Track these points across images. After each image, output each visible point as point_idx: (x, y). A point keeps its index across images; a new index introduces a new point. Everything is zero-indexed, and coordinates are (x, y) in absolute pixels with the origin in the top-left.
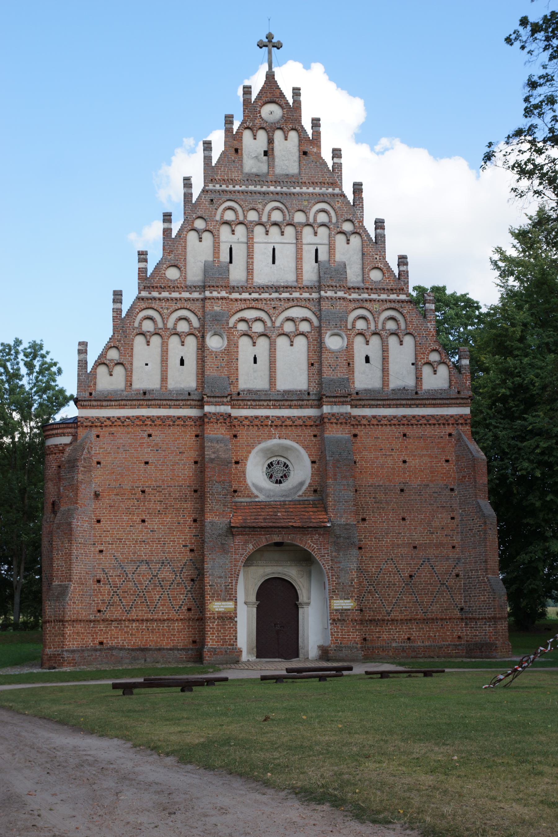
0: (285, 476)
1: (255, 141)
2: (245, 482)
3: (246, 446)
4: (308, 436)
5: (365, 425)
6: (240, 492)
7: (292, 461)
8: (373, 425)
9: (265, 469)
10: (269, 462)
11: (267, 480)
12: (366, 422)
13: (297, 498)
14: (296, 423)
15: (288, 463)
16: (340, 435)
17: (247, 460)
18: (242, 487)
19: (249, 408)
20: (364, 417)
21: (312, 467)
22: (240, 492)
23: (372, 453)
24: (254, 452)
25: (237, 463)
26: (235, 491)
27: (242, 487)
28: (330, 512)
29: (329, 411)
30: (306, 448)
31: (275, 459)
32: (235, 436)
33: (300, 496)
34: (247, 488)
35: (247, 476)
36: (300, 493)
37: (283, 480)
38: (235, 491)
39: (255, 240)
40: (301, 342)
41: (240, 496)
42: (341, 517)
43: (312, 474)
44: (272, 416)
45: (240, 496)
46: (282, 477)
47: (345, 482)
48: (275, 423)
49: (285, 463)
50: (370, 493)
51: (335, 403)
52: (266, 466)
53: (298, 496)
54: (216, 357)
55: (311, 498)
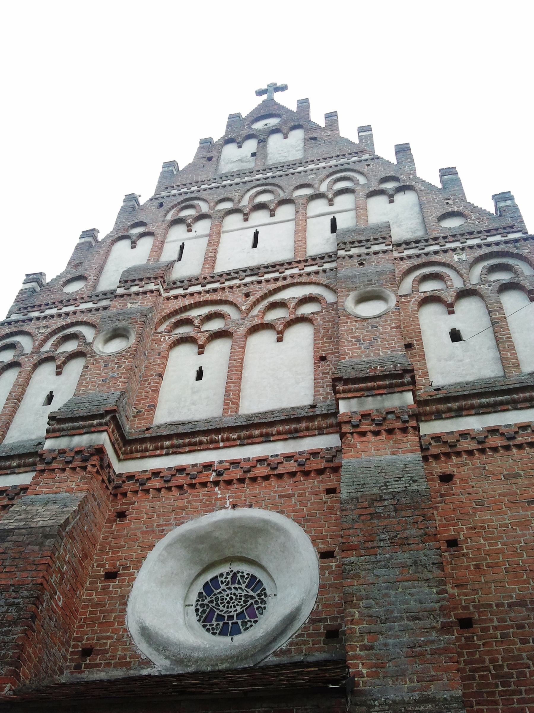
0: (252, 611)
1: (240, 149)
2: (123, 623)
3: (143, 533)
4: (312, 494)
5: (470, 453)
6: (99, 652)
7: (271, 567)
8: (495, 449)
9: (193, 597)
10: (208, 577)
11: (198, 626)
12: (472, 446)
13: (271, 659)
14: (281, 470)
15: (260, 575)
16: (390, 457)
17: (138, 568)
18: (108, 638)
19: (167, 454)
20: (464, 435)
21: (322, 569)
22: (99, 652)
23: (505, 513)
24: (161, 546)
25: (111, 576)
26: (87, 652)
27: (108, 638)
28: (355, 657)
29: (355, 410)
30: (303, 521)
31: (224, 569)
32: (122, 515)
33: (282, 652)
34: (123, 638)
35: (129, 608)
36: (283, 643)
37: (244, 623)
38: (87, 652)
39: (224, 229)
40: (301, 338)
41: (98, 665)
42: (399, 675)
43: (321, 586)
44: (221, 462)
45: (98, 665)
46: (240, 615)
47: (404, 557)
48: (226, 476)
49: (253, 577)
50: (522, 627)
51: (371, 392)
52: (198, 587)
53: (275, 654)
54: (106, 365)
55: (319, 656)
